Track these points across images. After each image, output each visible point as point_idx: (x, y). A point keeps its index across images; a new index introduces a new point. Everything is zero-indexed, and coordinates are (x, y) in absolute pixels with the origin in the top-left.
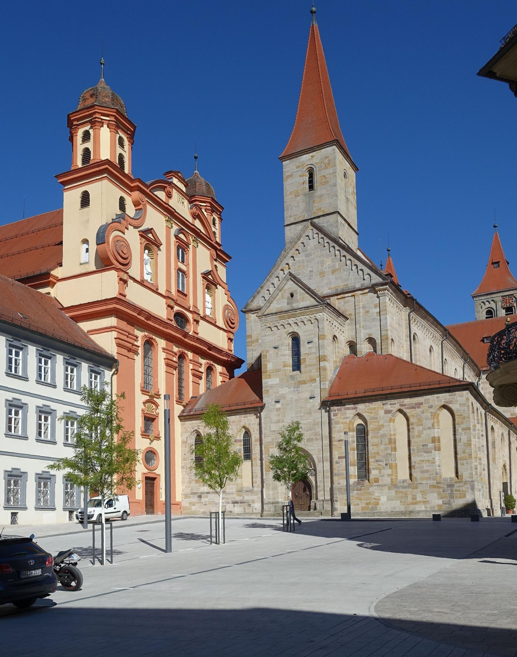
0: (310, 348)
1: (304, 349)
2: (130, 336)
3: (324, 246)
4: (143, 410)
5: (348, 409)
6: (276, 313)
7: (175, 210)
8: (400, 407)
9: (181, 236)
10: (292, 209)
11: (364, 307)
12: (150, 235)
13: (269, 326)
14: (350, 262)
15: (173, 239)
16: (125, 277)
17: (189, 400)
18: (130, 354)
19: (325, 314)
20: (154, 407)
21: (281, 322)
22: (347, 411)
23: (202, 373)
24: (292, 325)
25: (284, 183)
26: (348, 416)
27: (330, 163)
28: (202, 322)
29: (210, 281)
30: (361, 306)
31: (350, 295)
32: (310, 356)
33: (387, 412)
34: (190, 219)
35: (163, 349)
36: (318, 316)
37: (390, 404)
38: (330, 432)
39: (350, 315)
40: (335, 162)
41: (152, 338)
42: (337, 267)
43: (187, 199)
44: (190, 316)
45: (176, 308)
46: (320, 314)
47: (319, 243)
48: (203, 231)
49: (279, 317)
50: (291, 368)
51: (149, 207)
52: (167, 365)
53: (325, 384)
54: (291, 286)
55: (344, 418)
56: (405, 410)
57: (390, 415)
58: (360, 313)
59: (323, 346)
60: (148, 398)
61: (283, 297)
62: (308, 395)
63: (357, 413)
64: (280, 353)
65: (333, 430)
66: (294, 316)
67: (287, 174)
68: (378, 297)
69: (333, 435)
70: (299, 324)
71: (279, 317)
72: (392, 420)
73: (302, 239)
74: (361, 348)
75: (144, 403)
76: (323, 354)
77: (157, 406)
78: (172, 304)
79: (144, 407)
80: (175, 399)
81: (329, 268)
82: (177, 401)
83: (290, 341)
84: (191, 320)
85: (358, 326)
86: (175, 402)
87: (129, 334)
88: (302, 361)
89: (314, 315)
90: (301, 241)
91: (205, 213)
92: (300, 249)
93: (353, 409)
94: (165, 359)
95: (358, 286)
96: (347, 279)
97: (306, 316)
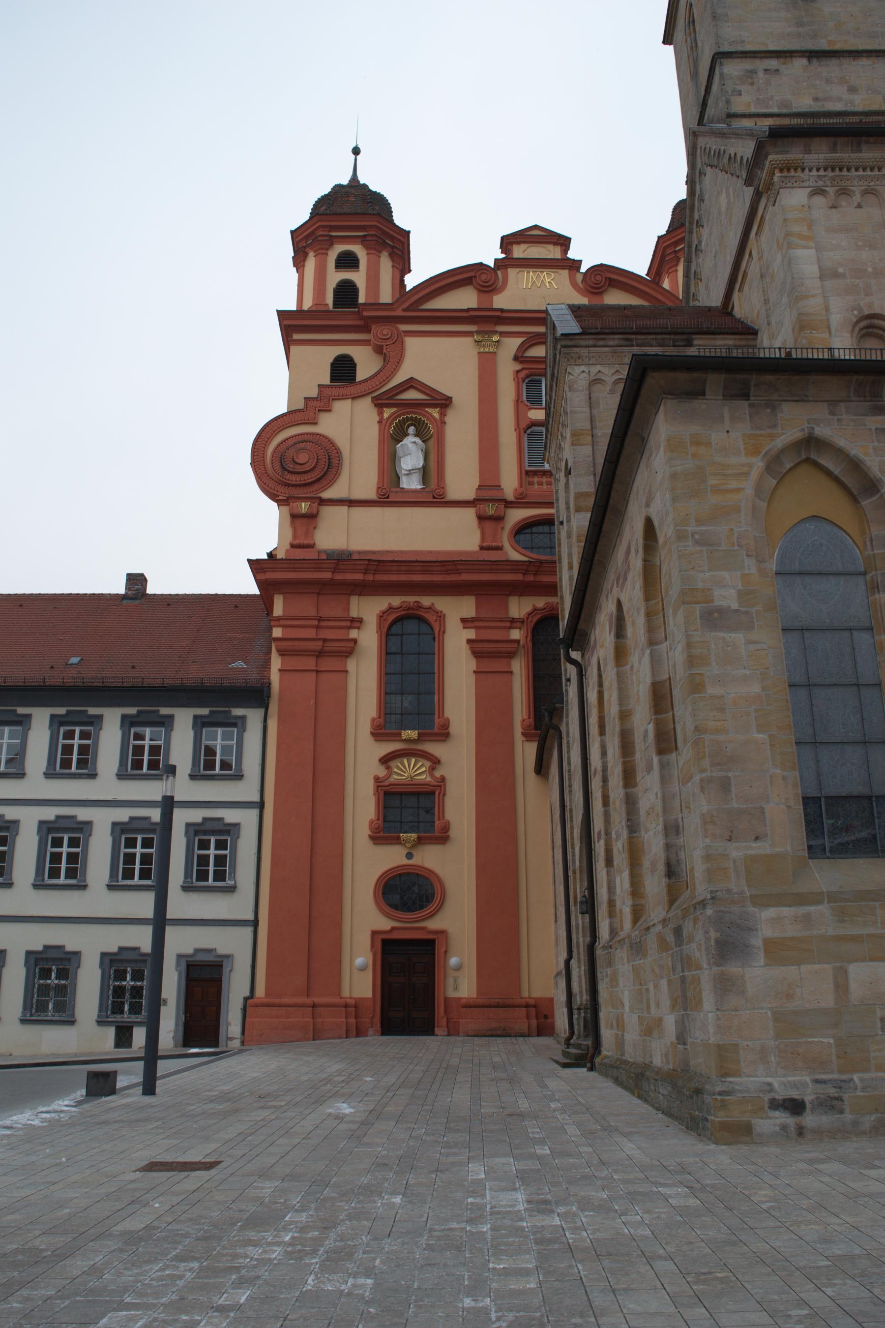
4: (377, 779)
12: (412, 395)
18: (327, 664)
41: (419, 606)
45: (517, 515)
52: (477, 654)
75: (385, 760)
80: (518, 730)
82: (523, 734)
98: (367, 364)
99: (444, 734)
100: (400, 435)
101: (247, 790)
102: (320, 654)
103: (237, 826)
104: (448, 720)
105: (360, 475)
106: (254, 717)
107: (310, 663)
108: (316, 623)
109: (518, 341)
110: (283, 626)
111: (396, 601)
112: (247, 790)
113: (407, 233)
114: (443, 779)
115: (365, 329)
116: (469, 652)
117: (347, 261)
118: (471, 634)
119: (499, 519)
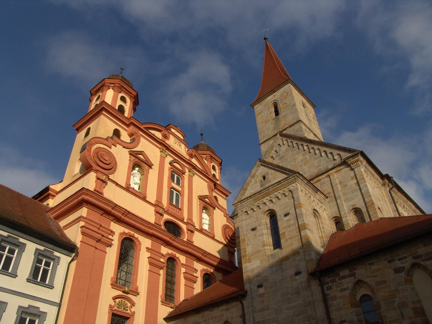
0: (288, 220)
1: (282, 223)
2: (101, 228)
3: (294, 147)
4: (110, 306)
5: (344, 277)
6: (250, 197)
7: (170, 146)
8: (414, 261)
9: (175, 164)
10: (264, 132)
11: (341, 183)
12: (141, 156)
13: (246, 210)
14: (318, 151)
15: (167, 166)
16: (104, 178)
17: (179, 303)
18: (99, 245)
19: (299, 185)
20: (129, 305)
21: (256, 204)
22: (343, 280)
23: (198, 277)
24: (268, 204)
25: (257, 119)
26: (345, 286)
27: (289, 94)
28: (196, 233)
29: (208, 205)
30: (338, 182)
31: (325, 175)
32: (289, 229)
33: (397, 271)
34: (187, 157)
35: (147, 248)
36: (291, 187)
37: (399, 260)
38: (328, 313)
39: (329, 193)
40: (292, 92)
41: (134, 237)
42: (308, 159)
43: (184, 144)
44: (184, 227)
45: (166, 217)
46: (294, 185)
47: (289, 146)
48: (198, 165)
49: (254, 200)
50: (272, 248)
51: (142, 139)
52: (150, 263)
53: (310, 254)
54: (262, 170)
55: (342, 290)
56: (422, 263)
57: (403, 274)
58: (338, 189)
59: (302, 214)
60: (121, 293)
61: (256, 182)
62: (292, 271)
63: (356, 280)
64: (258, 234)
65: (331, 309)
66: (268, 194)
67: (258, 112)
68: (352, 169)
69: (332, 316)
70: (274, 200)
71: (254, 200)
72: (409, 281)
73: (275, 148)
74: (348, 221)
75: (114, 298)
76: (302, 222)
77: (133, 304)
78: (161, 211)
79: (113, 304)
80: (160, 300)
81: (301, 161)
82: (161, 302)
83: (267, 220)
84: (185, 230)
85: (339, 201)
86: (160, 303)
87: (100, 226)
88: (281, 236)
89: (288, 187)
90: (274, 150)
91: (206, 161)
92: (274, 156)
93: (350, 276)
94: (148, 258)
95: (330, 167)
96: (320, 165)
97: (280, 191)
98: (125, 137)
99: (136, 293)
100: (133, 169)
101: (54, 295)
102: (99, 241)
103: (45, 313)
104: (138, 287)
105: (120, 176)
106: (65, 259)
107: (93, 242)
108: (99, 226)
109: (172, 159)
110: (86, 222)
111: (127, 231)
112: (54, 295)
113: (139, 104)
114: (134, 313)
115: (128, 126)
116: (148, 262)
117: (123, 99)
118: (149, 255)
119: (162, 215)
